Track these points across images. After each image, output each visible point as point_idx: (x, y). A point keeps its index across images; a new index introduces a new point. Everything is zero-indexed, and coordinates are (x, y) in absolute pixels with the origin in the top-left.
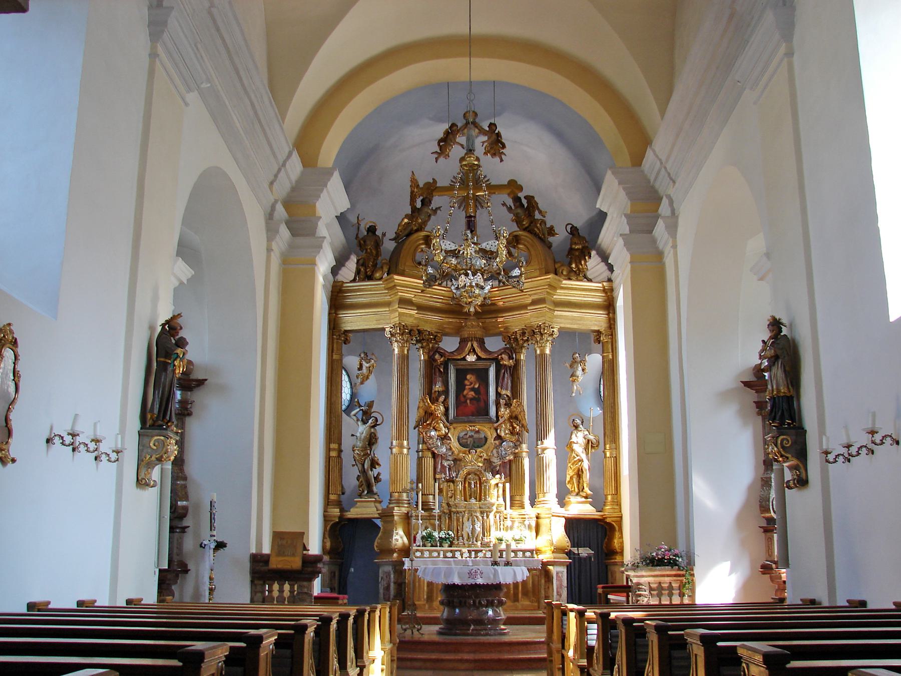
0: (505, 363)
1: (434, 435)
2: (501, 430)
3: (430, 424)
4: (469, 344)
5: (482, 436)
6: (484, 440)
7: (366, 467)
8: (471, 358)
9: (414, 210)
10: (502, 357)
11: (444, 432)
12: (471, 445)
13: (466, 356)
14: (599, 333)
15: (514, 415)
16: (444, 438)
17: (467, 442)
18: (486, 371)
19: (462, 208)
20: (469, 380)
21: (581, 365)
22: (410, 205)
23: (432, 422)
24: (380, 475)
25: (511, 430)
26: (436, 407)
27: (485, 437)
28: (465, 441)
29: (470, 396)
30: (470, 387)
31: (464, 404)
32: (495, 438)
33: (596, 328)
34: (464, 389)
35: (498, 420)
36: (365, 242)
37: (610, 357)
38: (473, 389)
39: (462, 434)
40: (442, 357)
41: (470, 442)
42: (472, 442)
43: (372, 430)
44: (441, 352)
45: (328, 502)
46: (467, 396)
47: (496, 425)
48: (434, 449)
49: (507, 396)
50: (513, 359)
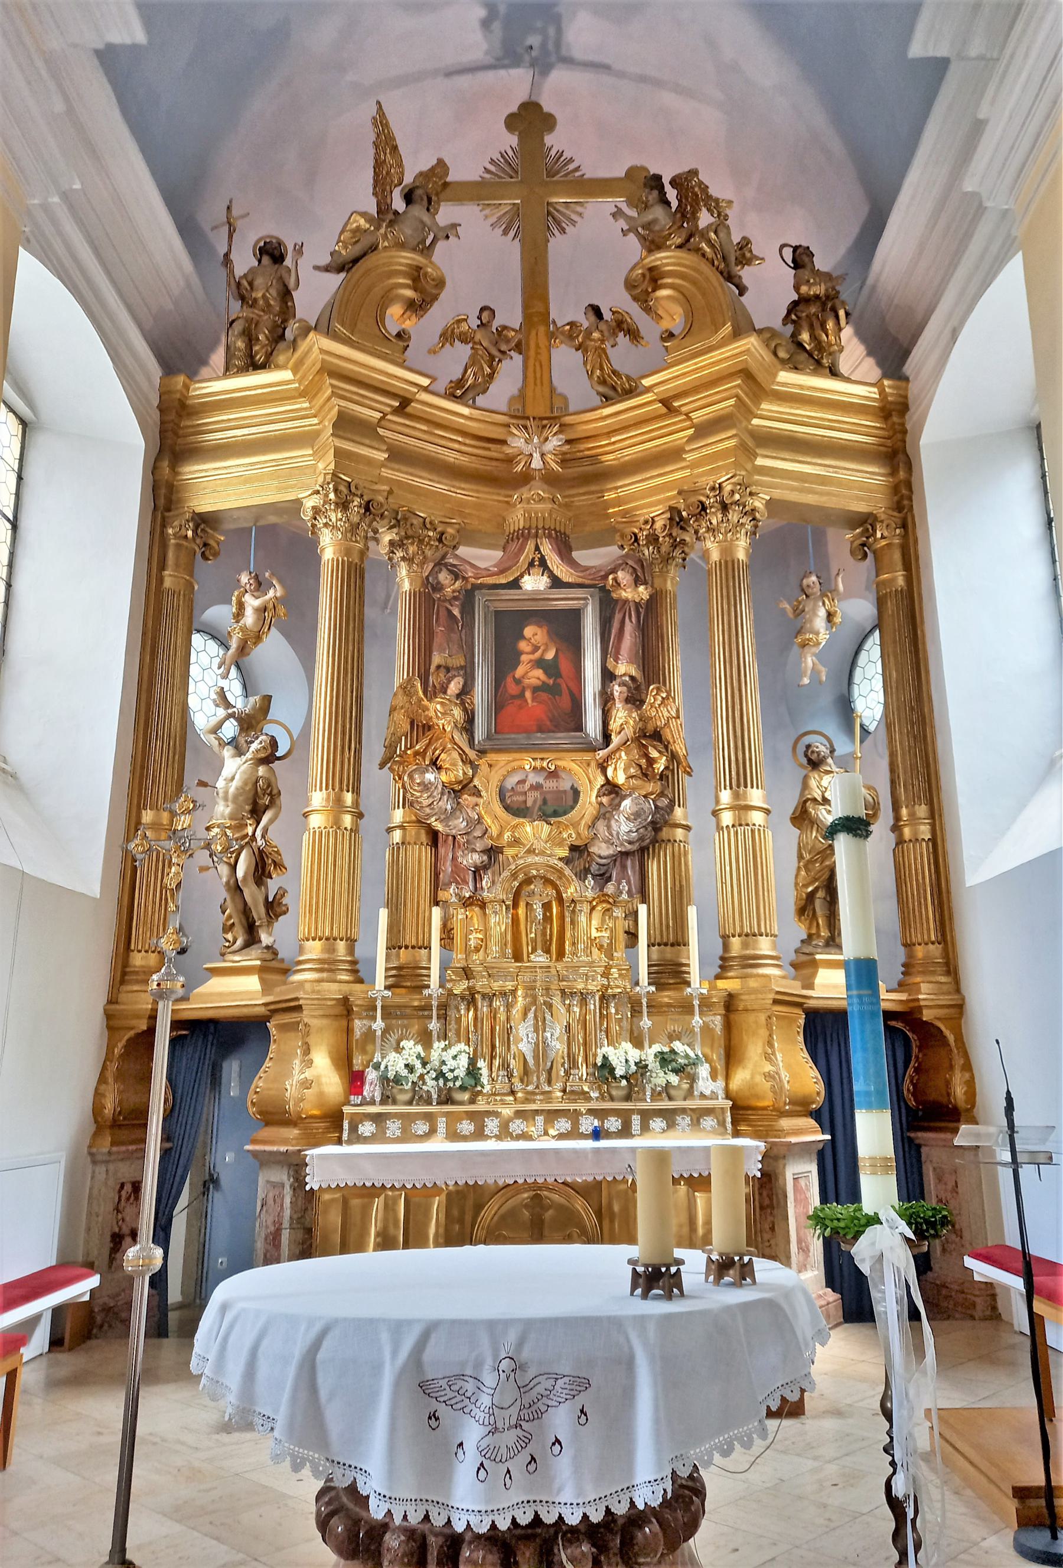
0: (624, 594)
1: (433, 780)
2: (615, 769)
3: (423, 754)
4: (530, 545)
5: (565, 785)
6: (571, 793)
7: (240, 872)
8: (534, 583)
9: (384, 208)
10: (615, 579)
11: (461, 774)
12: (536, 808)
13: (522, 576)
14: (866, 522)
15: (650, 727)
16: (459, 790)
17: (525, 802)
18: (574, 617)
19: (512, 233)
20: (529, 640)
21: (824, 604)
22: (375, 194)
23: (428, 746)
24: (283, 896)
25: (644, 766)
26: (439, 707)
27: (572, 788)
28: (521, 798)
29: (534, 682)
30: (531, 657)
31: (518, 702)
32: (599, 791)
33: (862, 507)
34: (517, 663)
35: (607, 737)
36: (251, 284)
37: (901, 582)
38: (540, 663)
39: (512, 781)
40: (456, 579)
41: (535, 801)
42: (539, 803)
43: (262, 770)
44: (454, 566)
45: (124, 974)
46: (526, 681)
47: (602, 754)
48: (433, 819)
49: (632, 678)
50: (645, 583)
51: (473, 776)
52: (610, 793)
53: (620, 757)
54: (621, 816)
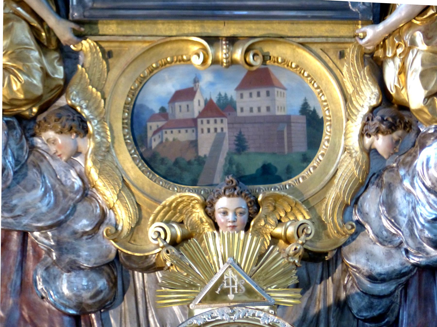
2: (403, 70)
11: (37, 81)
17: (194, 144)
32: (368, 119)
51: (67, 80)
52: (392, 128)
53: (413, 43)
54: (418, 182)
